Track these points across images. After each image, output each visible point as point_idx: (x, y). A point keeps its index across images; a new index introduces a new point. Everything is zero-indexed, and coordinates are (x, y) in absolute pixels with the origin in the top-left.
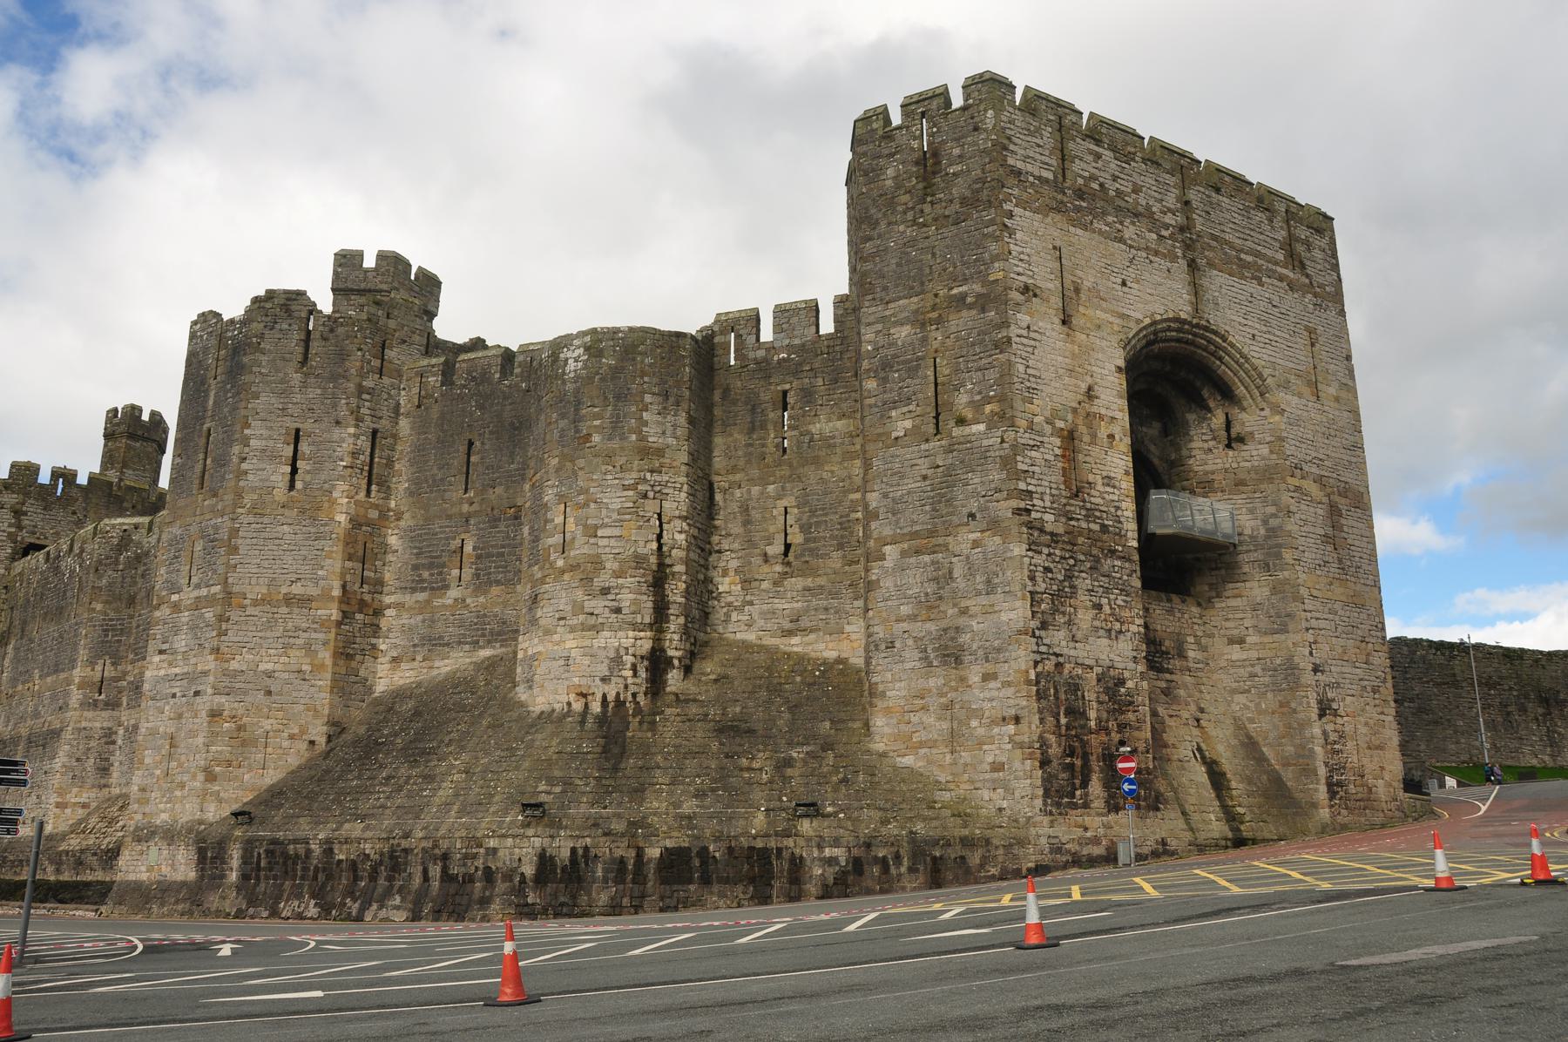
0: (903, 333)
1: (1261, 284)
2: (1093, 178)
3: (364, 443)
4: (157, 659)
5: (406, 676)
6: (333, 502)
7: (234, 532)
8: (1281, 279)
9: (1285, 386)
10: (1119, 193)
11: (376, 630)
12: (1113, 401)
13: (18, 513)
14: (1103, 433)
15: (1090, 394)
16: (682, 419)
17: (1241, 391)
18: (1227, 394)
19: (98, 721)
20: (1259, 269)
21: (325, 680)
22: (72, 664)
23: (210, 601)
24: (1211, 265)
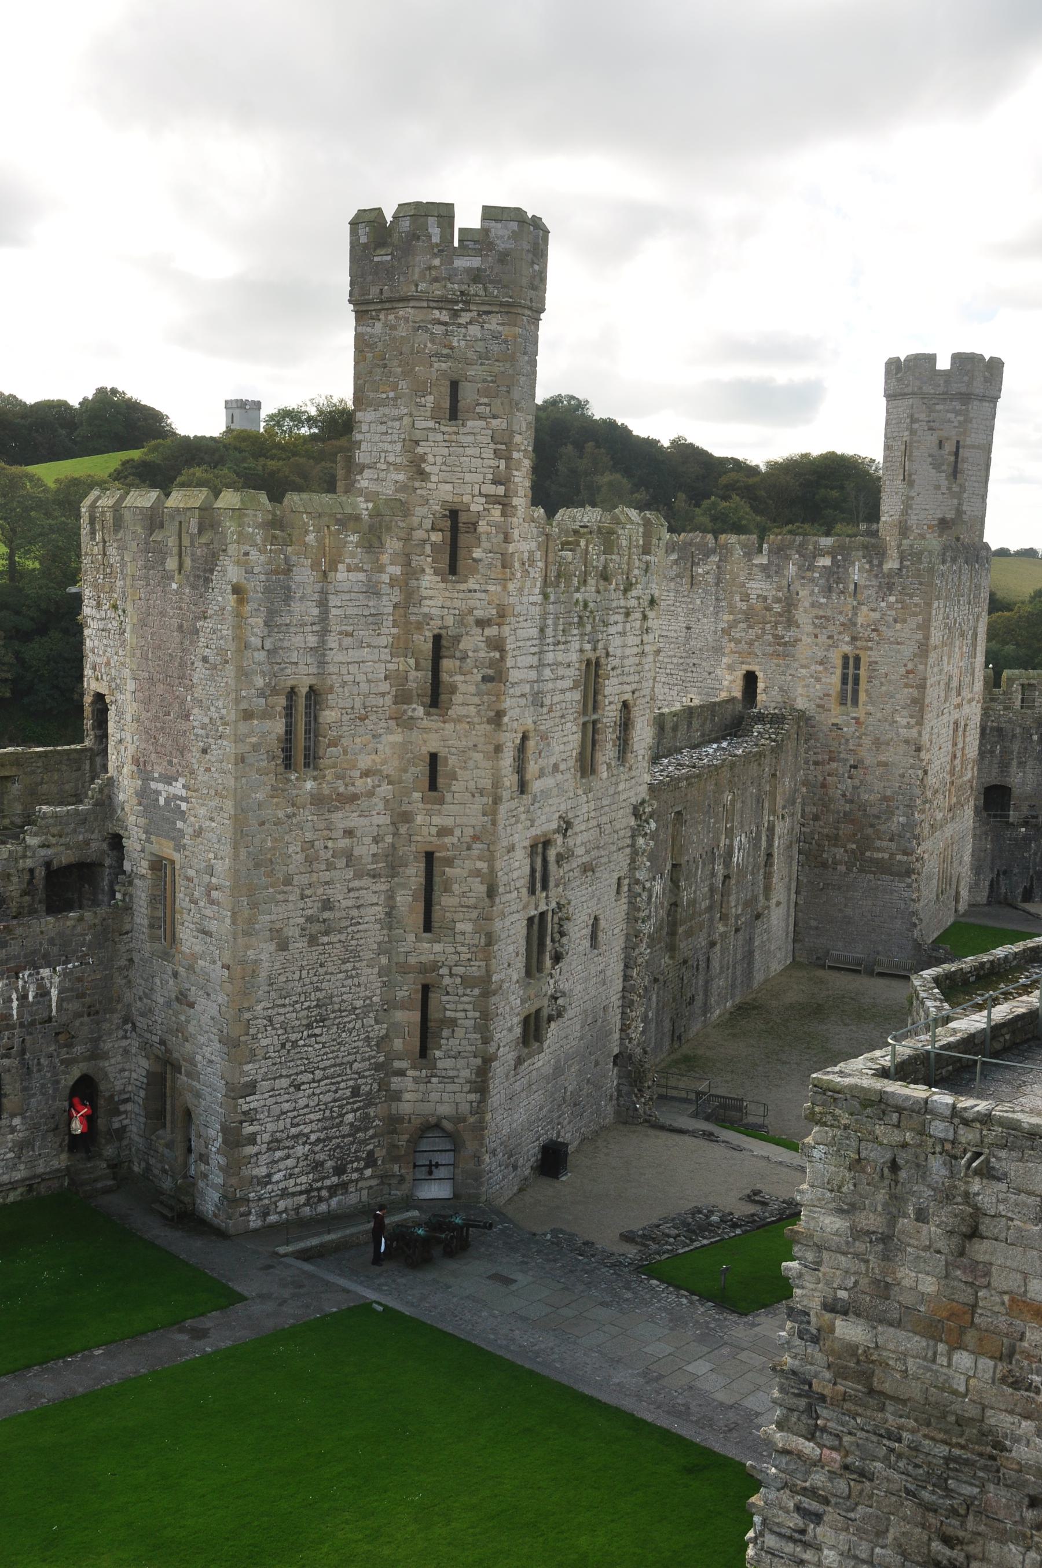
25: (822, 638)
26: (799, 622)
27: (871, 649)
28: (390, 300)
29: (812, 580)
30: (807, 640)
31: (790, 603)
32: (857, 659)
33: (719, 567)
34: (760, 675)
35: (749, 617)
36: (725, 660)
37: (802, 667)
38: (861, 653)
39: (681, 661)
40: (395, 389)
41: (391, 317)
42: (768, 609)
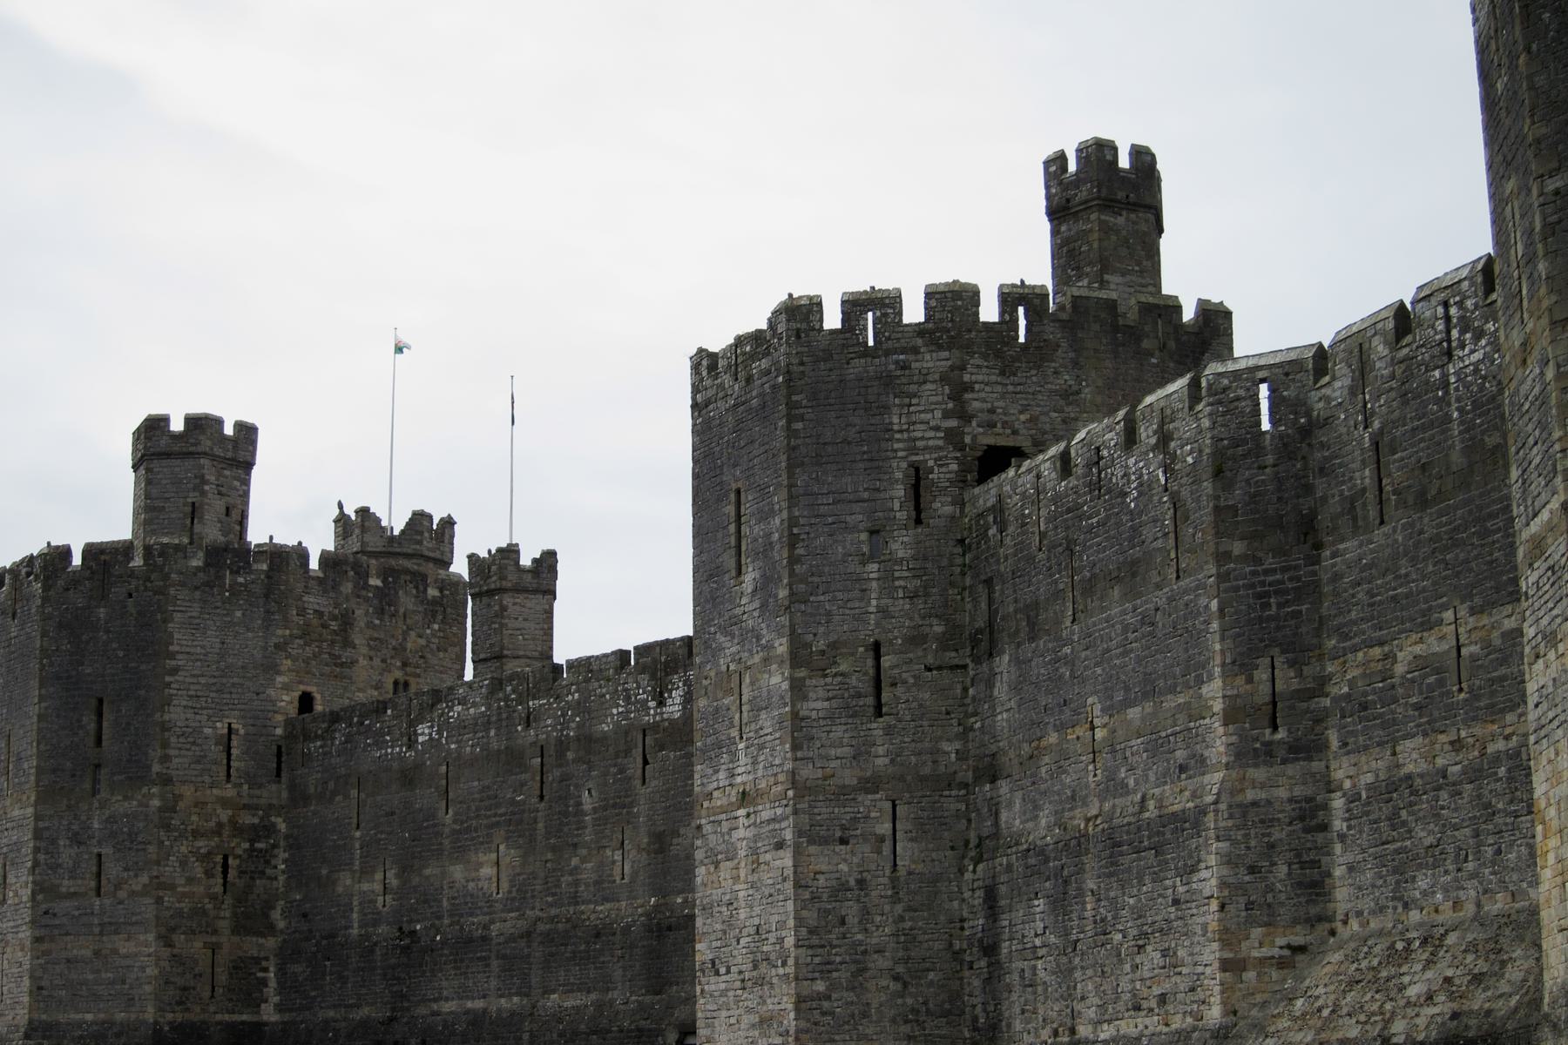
22: (1195, 673)
25: (377, 662)
26: (357, 642)
27: (419, 676)
28: (1134, 204)
29: (367, 600)
30: (363, 662)
31: (346, 621)
32: (406, 684)
33: (268, 577)
34: (318, 696)
35: (305, 633)
36: (279, 679)
37: (360, 690)
38: (412, 680)
39: (213, 681)
40: (1139, 263)
41: (1133, 216)
42: (324, 626)
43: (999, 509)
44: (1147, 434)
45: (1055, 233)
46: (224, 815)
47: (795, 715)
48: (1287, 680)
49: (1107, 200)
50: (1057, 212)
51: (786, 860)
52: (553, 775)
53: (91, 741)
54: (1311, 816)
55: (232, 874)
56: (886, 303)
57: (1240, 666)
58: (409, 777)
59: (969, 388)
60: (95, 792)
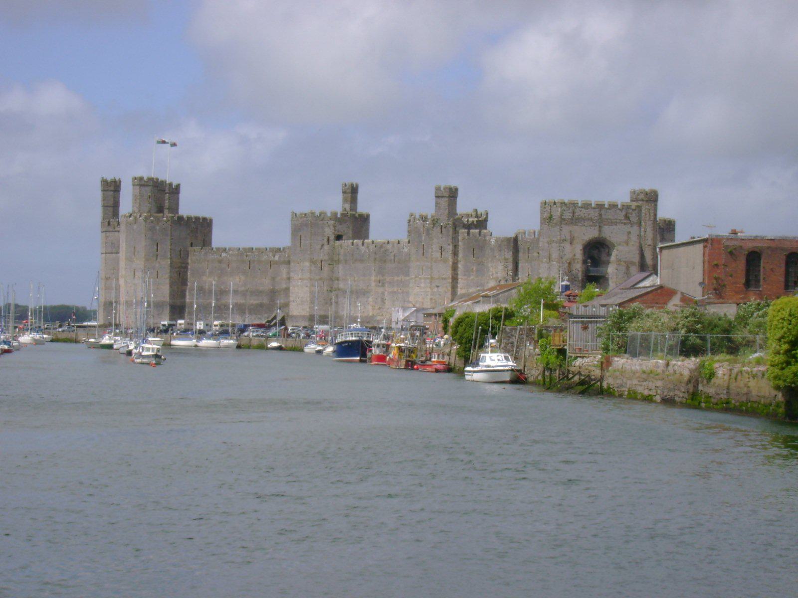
0: (546, 245)
1: (616, 225)
2: (579, 215)
3: (454, 248)
4: (417, 288)
5: (464, 291)
6: (449, 260)
7: (432, 266)
8: (622, 223)
9: (619, 245)
10: (585, 217)
11: (457, 283)
12: (579, 256)
13: (335, 227)
14: (576, 261)
15: (574, 255)
16: (511, 253)
17: (610, 246)
18: (608, 247)
19: (380, 290)
20: (616, 222)
21: (450, 293)
23: (427, 278)
24: (604, 225)
31: (197, 228)
43: (341, 246)
44: (365, 245)
45: (343, 195)
46: (179, 265)
47: (310, 269)
48: (381, 278)
49: (352, 192)
50: (344, 192)
51: (307, 289)
52: (252, 266)
53: (156, 250)
54: (383, 293)
55: (181, 275)
56: (325, 213)
57: (376, 276)
58: (220, 262)
59: (336, 226)
60: (157, 259)
